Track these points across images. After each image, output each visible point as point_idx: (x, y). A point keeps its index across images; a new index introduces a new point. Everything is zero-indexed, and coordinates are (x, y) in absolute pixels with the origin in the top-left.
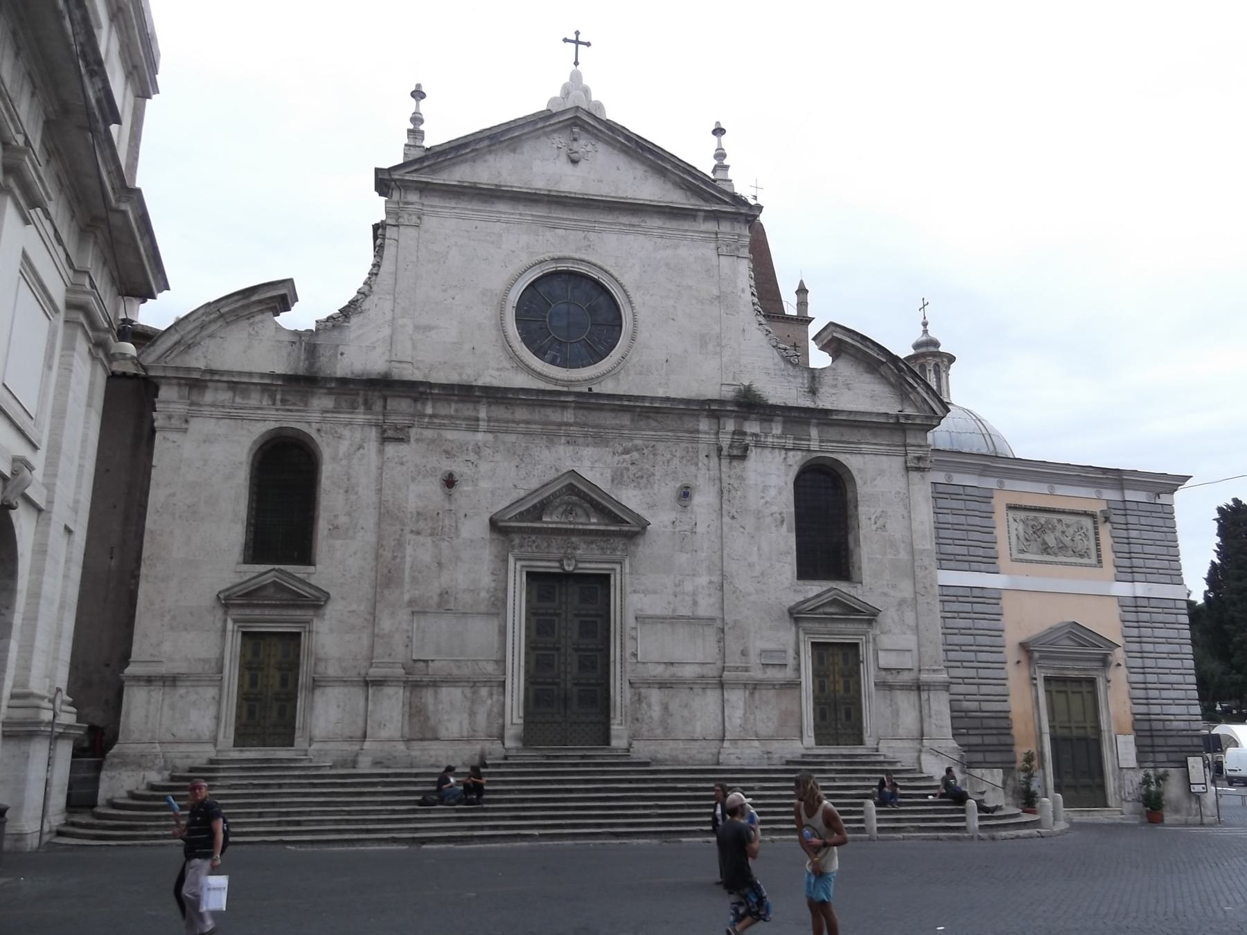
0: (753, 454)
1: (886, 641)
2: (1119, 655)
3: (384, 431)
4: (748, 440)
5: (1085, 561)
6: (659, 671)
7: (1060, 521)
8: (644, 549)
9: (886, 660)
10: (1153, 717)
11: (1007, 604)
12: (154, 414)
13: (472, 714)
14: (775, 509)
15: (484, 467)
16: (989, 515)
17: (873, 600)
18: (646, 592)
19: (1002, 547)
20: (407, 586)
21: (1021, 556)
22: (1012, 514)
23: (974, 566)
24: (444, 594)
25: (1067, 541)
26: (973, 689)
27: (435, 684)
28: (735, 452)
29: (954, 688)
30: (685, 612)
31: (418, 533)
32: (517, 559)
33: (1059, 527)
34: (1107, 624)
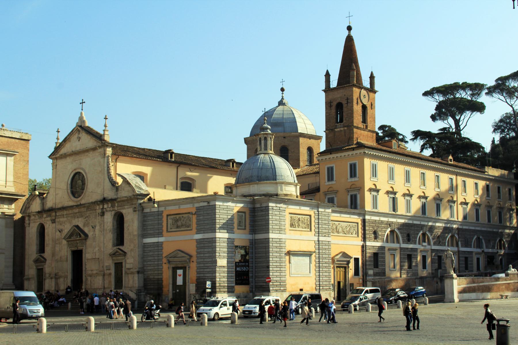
0: (105, 214)
1: (128, 261)
2: (194, 259)
3: (51, 221)
4: (104, 210)
5: (189, 229)
6: (90, 272)
7: (183, 217)
8: (89, 242)
9: (128, 266)
10: (201, 278)
11: (164, 246)
12: (25, 224)
13: (64, 284)
14: (109, 228)
15: (66, 226)
17: (125, 250)
18: (89, 253)
20: (56, 256)
21: (171, 230)
22: (169, 217)
24: (61, 257)
25: (184, 223)
26: (153, 272)
27: (59, 278)
28: (102, 214)
30: (94, 257)
31: (57, 244)
32: (70, 248)
33: (182, 219)
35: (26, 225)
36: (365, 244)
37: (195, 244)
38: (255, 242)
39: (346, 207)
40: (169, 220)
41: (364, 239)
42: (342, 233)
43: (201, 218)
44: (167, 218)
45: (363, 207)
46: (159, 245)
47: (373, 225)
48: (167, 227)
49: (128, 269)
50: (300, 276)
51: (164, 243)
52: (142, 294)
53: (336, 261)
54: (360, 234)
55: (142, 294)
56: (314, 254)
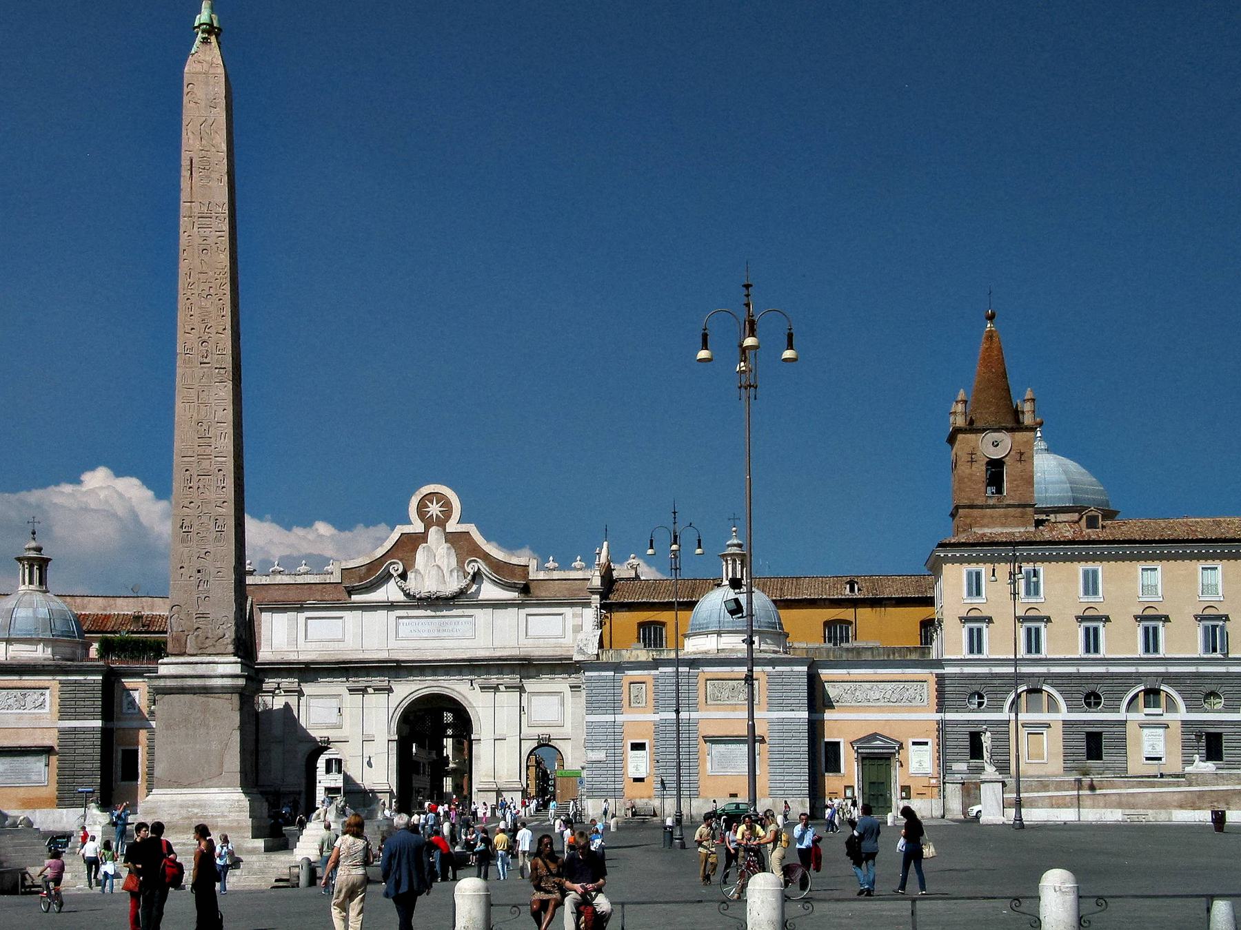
41: (941, 708)
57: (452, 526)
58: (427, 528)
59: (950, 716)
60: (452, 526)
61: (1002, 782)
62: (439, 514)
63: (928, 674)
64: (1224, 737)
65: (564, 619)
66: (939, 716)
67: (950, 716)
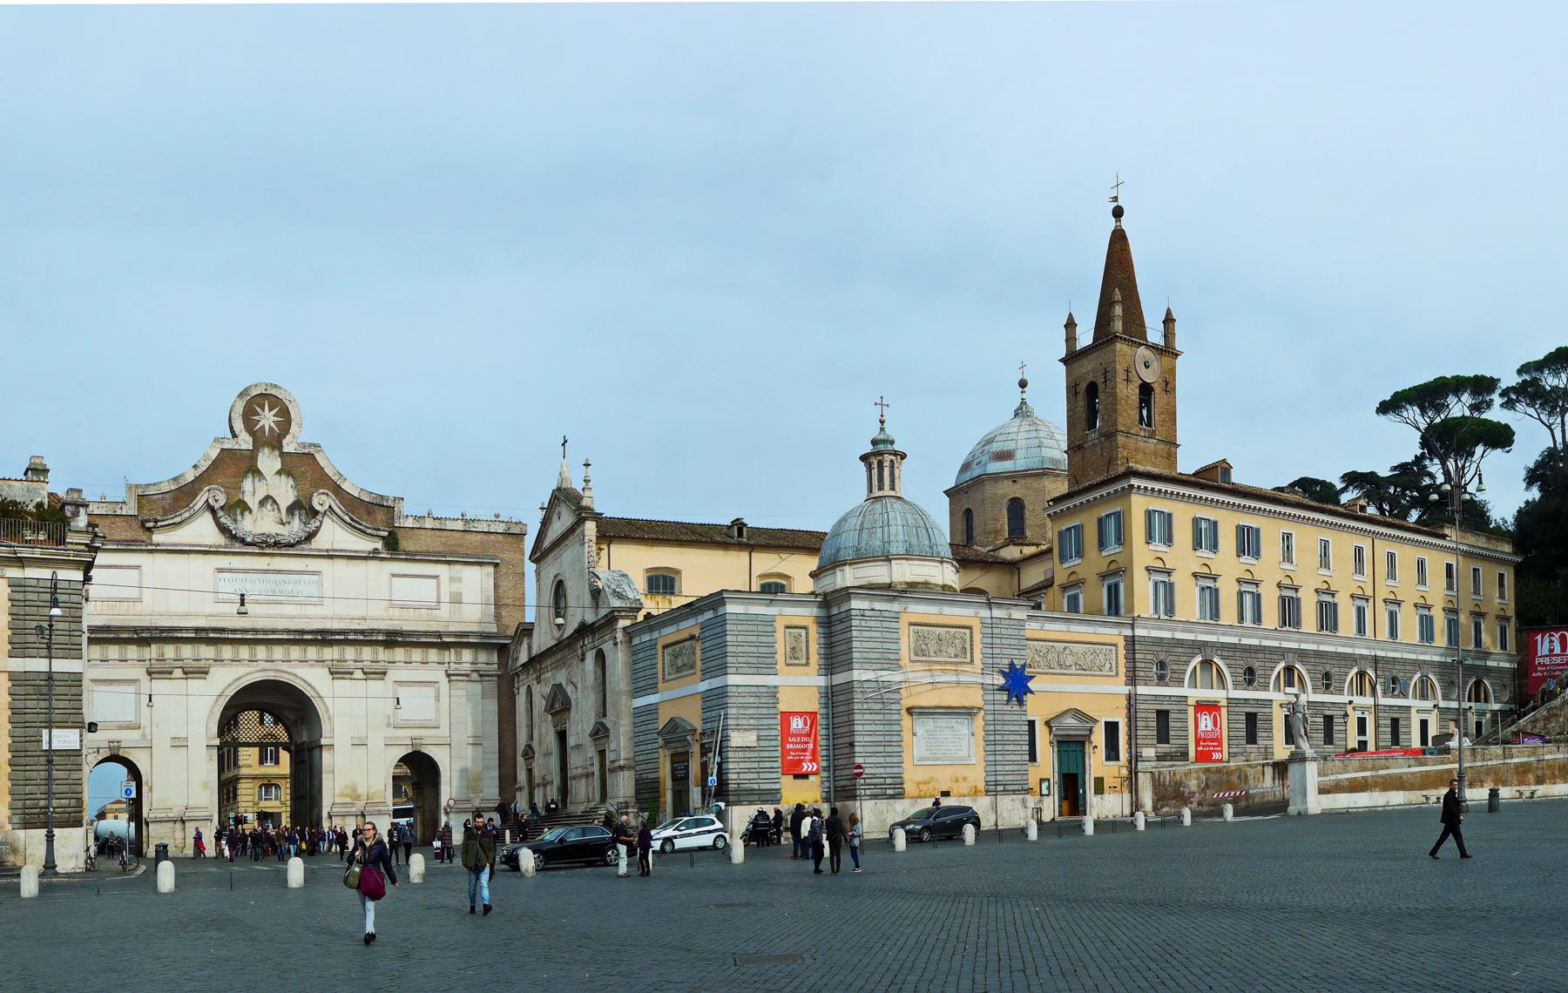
1: (613, 746)
16: (654, 656)
19: (660, 676)
21: (670, 677)
22: (666, 651)
23: (648, 691)
25: (686, 661)
29: (637, 768)
33: (684, 651)
34: (693, 717)
35: (516, 692)
36: (1136, 691)
37: (700, 702)
38: (832, 693)
39: (1100, 613)
40: (666, 657)
41: (1132, 680)
42: (1074, 666)
43: (707, 644)
44: (663, 652)
45: (1131, 609)
46: (652, 710)
47: (1154, 648)
48: (663, 671)
49: (612, 762)
50: (940, 763)
51: (660, 706)
52: (629, 810)
53: (1054, 729)
54: (1122, 670)
55: (629, 810)
56: (982, 713)
57: (289, 446)
58: (257, 445)
59: (1142, 690)
60: (289, 446)
61: (1151, 772)
62: (273, 425)
63: (1114, 635)
64: (1335, 720)
65: (438, 584)
66: (1126, 690)
67: (1142, 690)
